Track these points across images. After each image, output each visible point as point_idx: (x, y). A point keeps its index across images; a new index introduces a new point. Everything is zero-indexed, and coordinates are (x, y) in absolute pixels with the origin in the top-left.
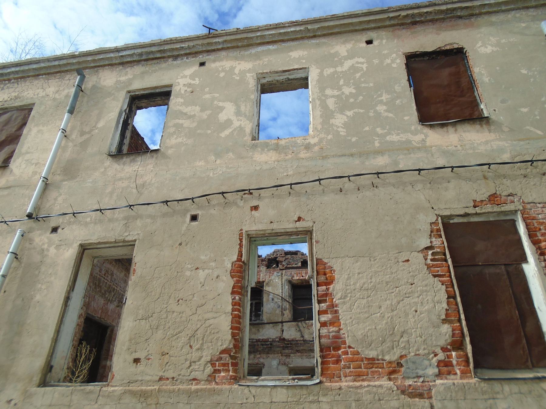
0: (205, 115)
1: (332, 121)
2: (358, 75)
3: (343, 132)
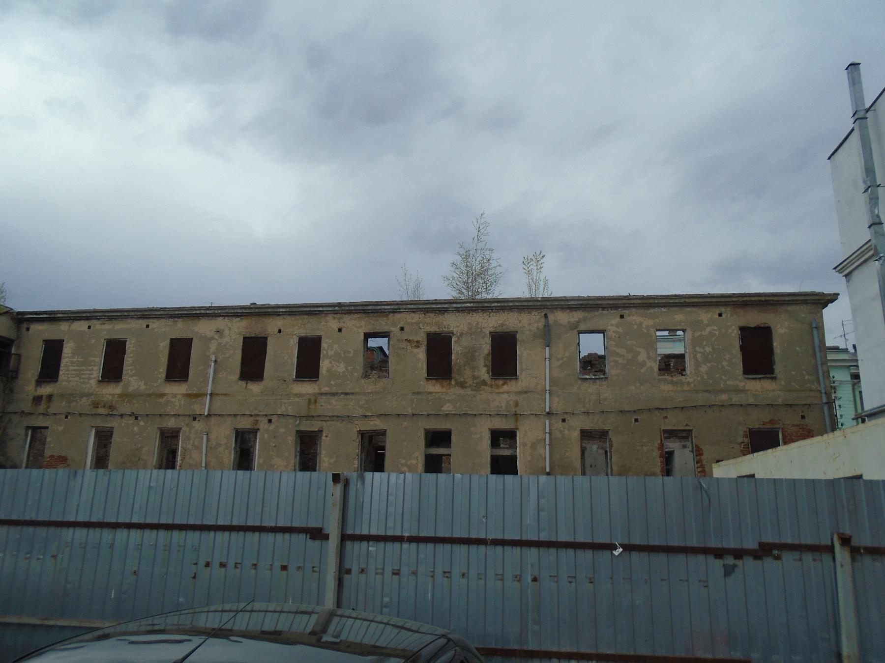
0: (630, 356)
1: (700, 369)
2: (713, 339)
3: (705, 377)
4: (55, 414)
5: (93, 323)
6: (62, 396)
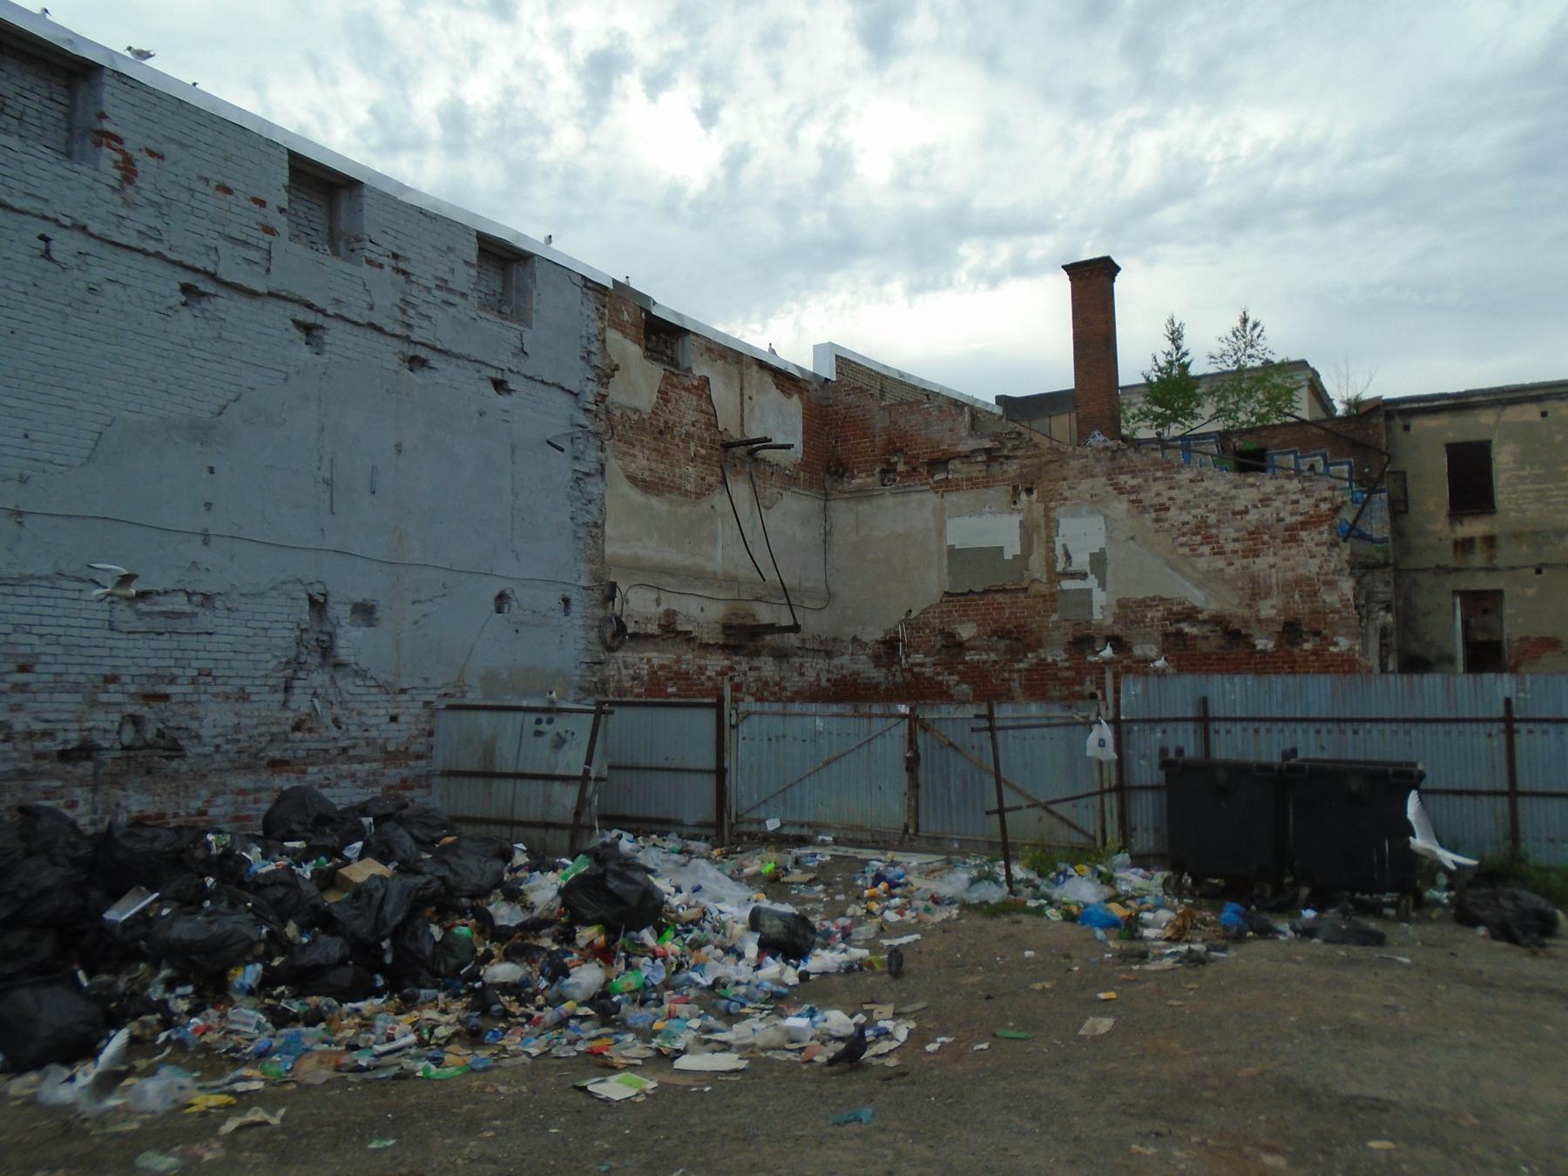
4: (1513, 568)
5: (1547, 406)
6: (1517, 537)
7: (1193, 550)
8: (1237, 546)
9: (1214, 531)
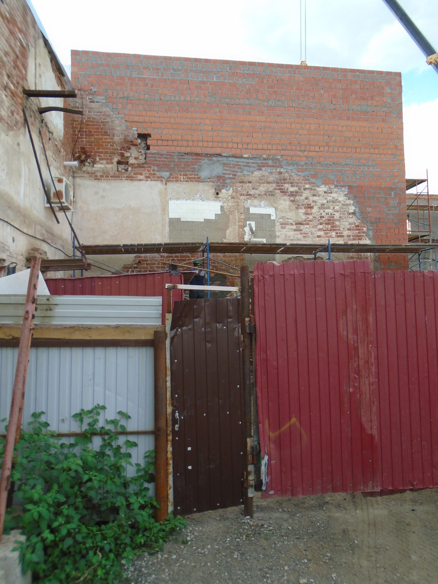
7: (325, 234)
8: (350, 233)
9: (337, 223)
